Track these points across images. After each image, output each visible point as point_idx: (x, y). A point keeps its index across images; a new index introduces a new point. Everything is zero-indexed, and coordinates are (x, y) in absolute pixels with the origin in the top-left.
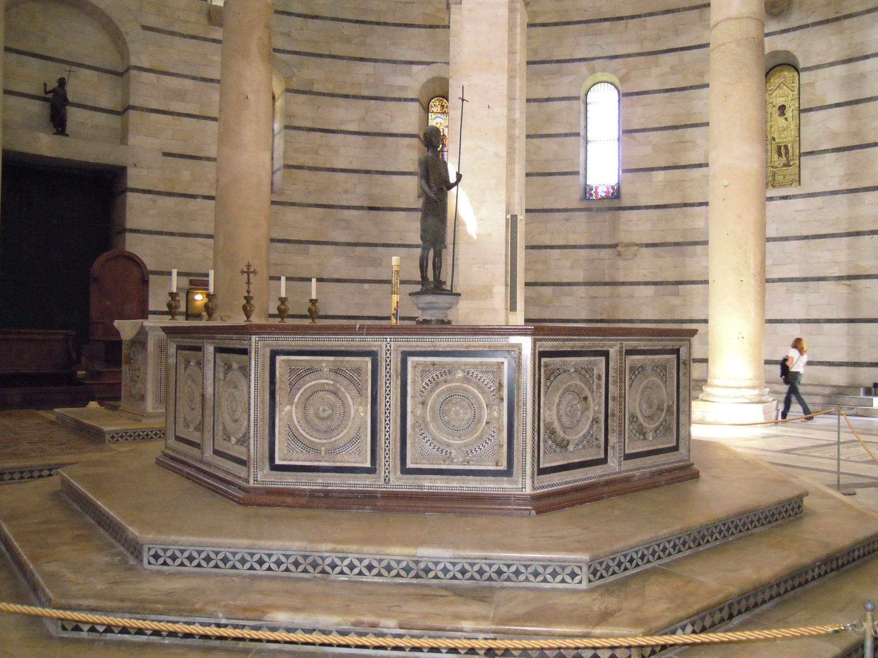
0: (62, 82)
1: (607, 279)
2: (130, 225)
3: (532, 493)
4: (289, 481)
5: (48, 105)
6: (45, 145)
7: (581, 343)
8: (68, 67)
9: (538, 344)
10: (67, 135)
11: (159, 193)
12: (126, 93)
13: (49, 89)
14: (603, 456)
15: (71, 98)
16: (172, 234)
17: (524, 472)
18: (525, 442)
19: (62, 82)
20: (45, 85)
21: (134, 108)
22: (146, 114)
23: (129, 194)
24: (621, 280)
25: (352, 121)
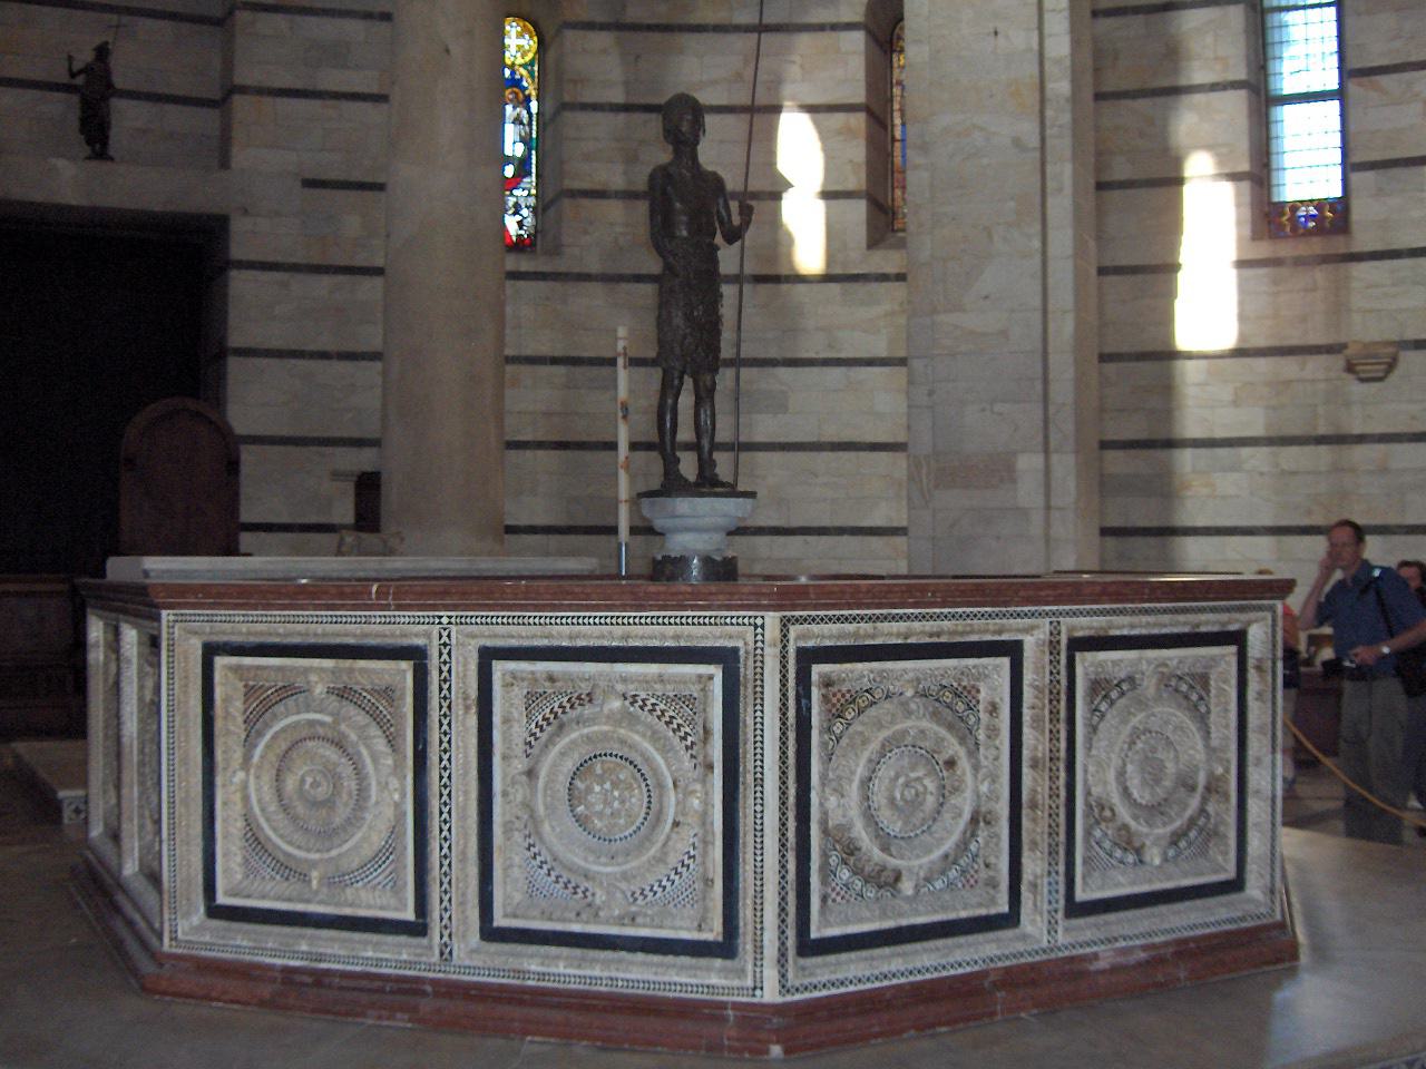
0: (102, 52)
1: (1322, 430)
2: (235, 339)
3: (779, 999)
4: (242, 943)
5: (75, 99)
6: (66, 181)
7: (929, 626)
8: (114, 18)
9: (794, 630)
10: (112, 159)
11: (295, 268)
12: (228, 65)
13: (77, 66)
14: (1005, 909)
15: (119, 81)
16: (324, 355)
17: (759, 948)
18: (759, 874)
19: (102, 52)
20: (70, 59)
21: (243, 90)
22: (267, 101)
23: (234, 273)
24: (1357, 431)
25: (713, 83)
